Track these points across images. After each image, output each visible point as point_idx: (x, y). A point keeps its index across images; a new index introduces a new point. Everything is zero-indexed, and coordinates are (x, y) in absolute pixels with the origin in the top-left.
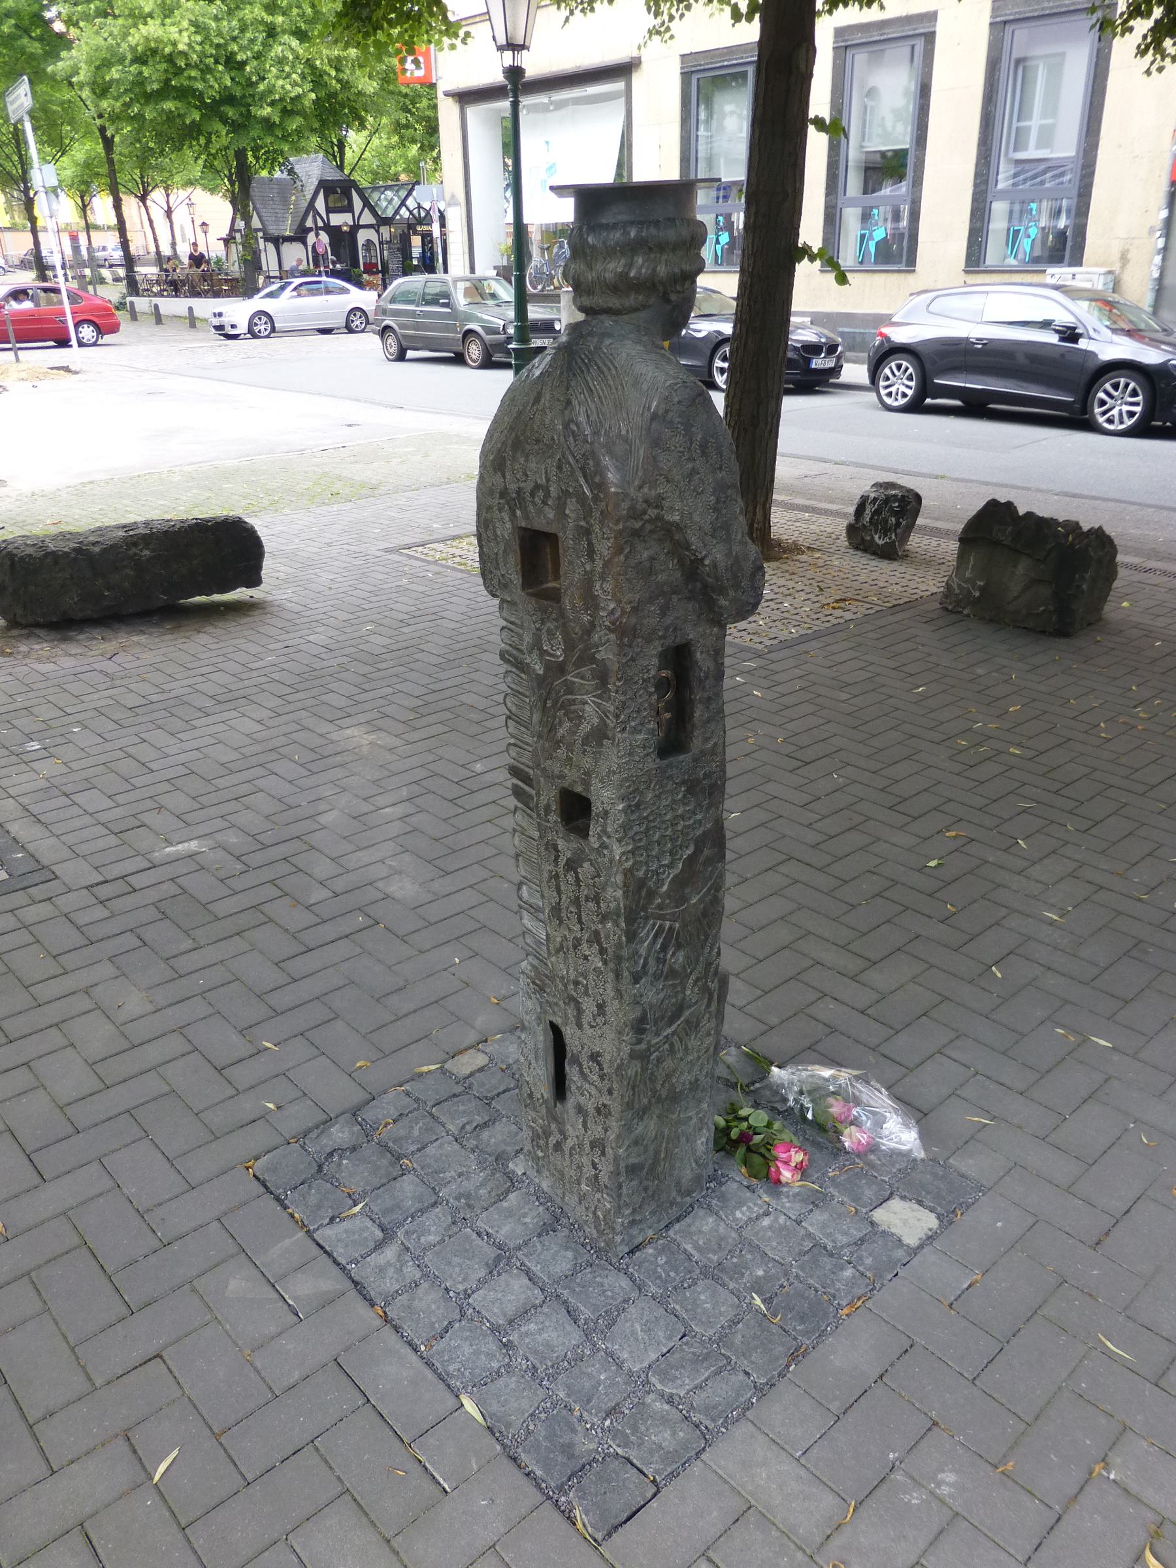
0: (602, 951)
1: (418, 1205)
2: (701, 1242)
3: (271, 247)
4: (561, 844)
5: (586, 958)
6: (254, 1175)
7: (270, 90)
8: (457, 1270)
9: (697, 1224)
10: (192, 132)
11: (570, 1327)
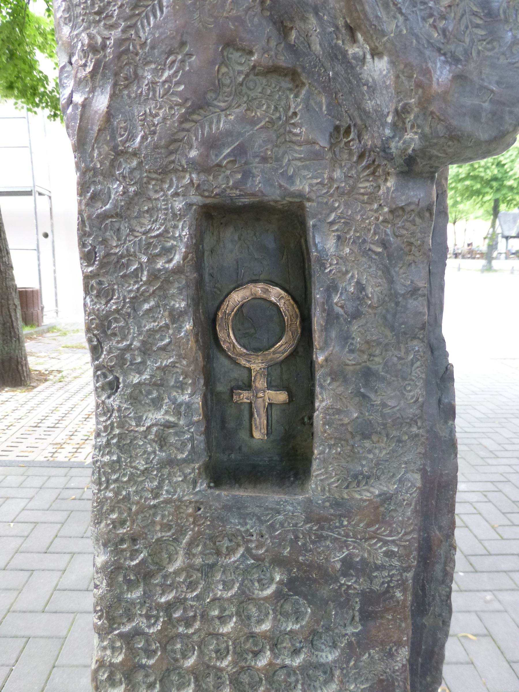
3: (504, 240)
10: (478, 193)
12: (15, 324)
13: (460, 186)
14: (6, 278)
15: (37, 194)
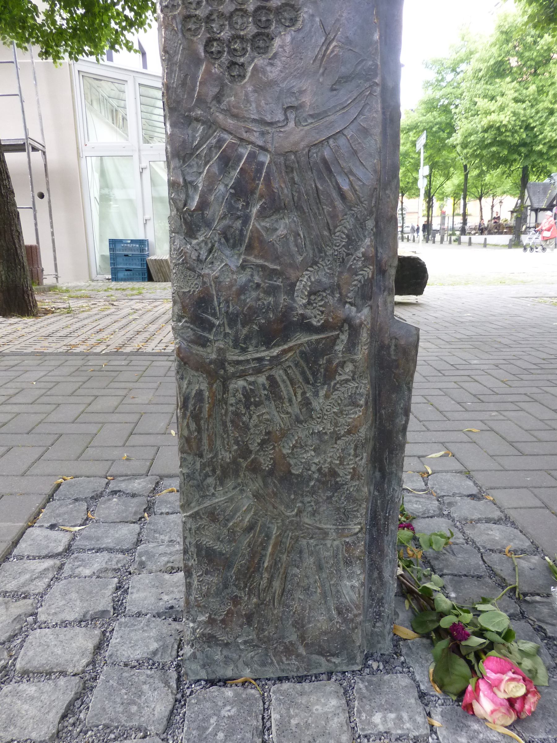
1: (111, 545)
2: (294, 722)
3: (533, 213)
6: (59, 485)
7: (545, 138)
8: (63, 602)
9: (313, 698)
10: (505, 161)
11: (54, 716)
12: (19, 252)
13: (484, 152)
14: (8, 202)
15: (30, 149)
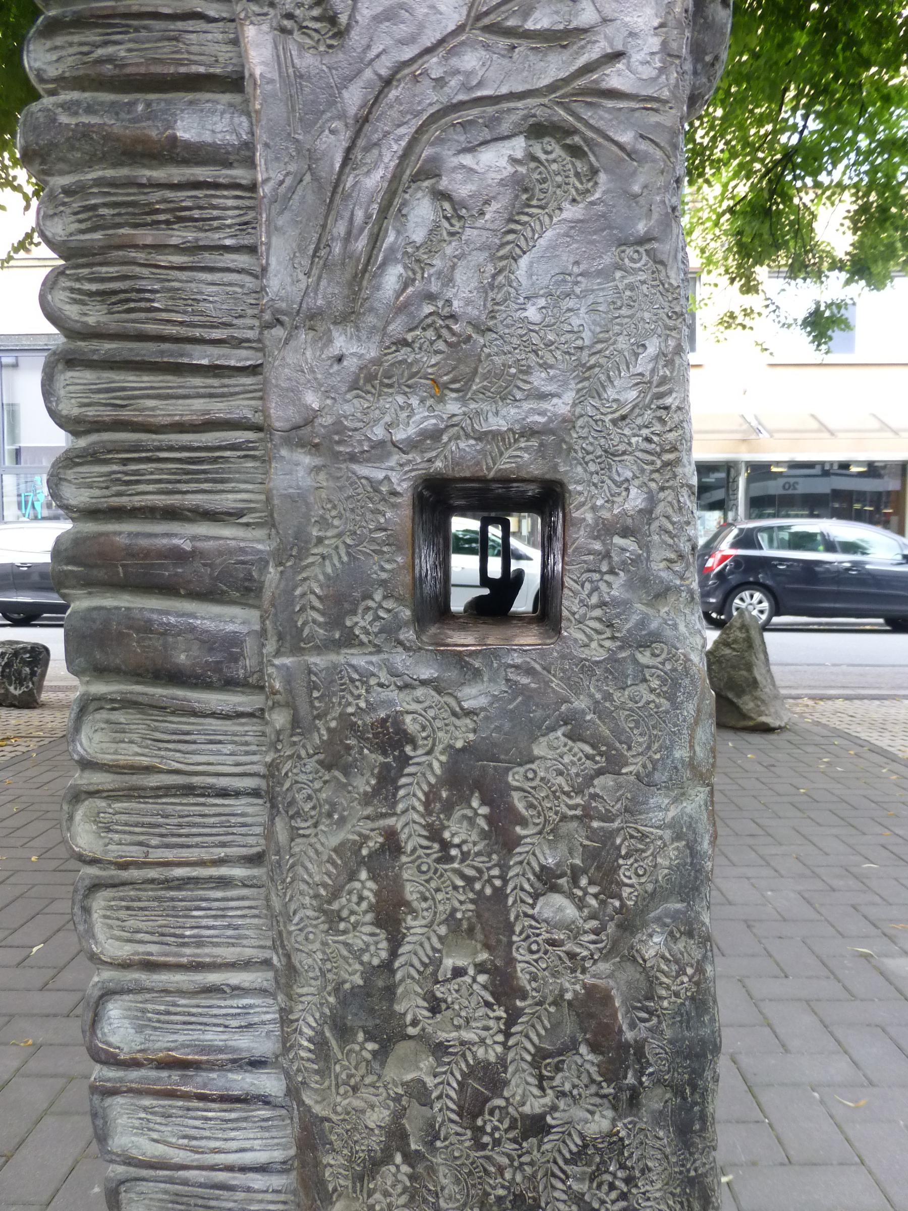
0: (618, 1057)
4: (412, 709)
5: (536, 1126)
